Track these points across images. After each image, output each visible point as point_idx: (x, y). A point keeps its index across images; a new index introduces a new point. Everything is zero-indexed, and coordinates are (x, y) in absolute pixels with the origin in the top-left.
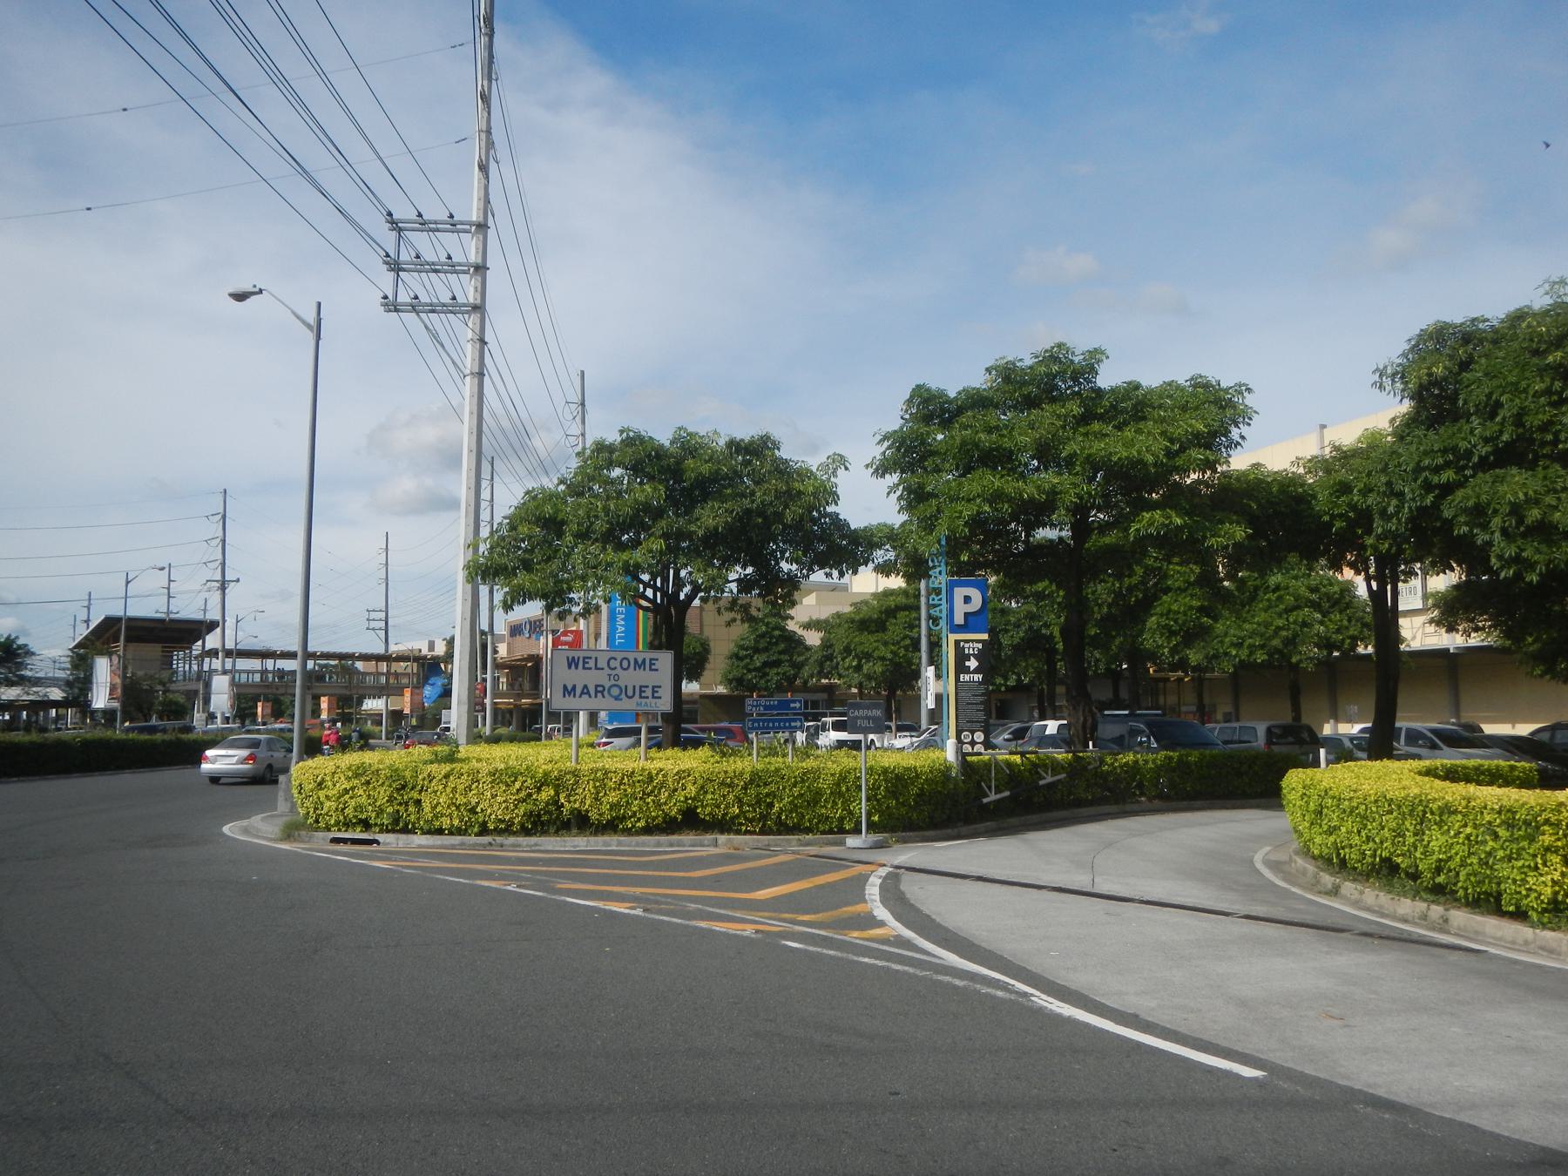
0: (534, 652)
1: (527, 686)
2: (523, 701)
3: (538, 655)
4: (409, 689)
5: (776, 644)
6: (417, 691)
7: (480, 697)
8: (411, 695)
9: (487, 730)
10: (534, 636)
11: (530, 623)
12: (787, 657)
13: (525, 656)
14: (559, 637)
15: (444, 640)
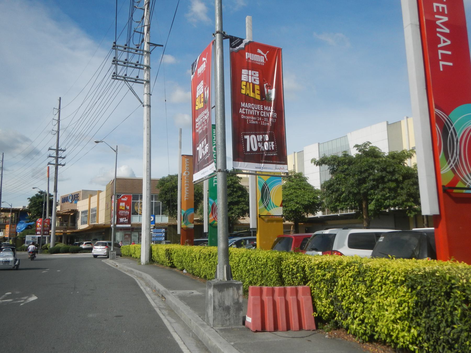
0: (75, 209)
1: (70, 224)
2: (68, 231)
3: (76, 210)
4: (9, 225)
5: (236, 192)
6: (13, 226)
7: (47, 227)
8: (10, 228)
9: (51, 245)
10: (74, 202)
11: (72, 196)
12: (243, 199)
13: (70, 210)
14: (242, 52)
15: (28, 199)
